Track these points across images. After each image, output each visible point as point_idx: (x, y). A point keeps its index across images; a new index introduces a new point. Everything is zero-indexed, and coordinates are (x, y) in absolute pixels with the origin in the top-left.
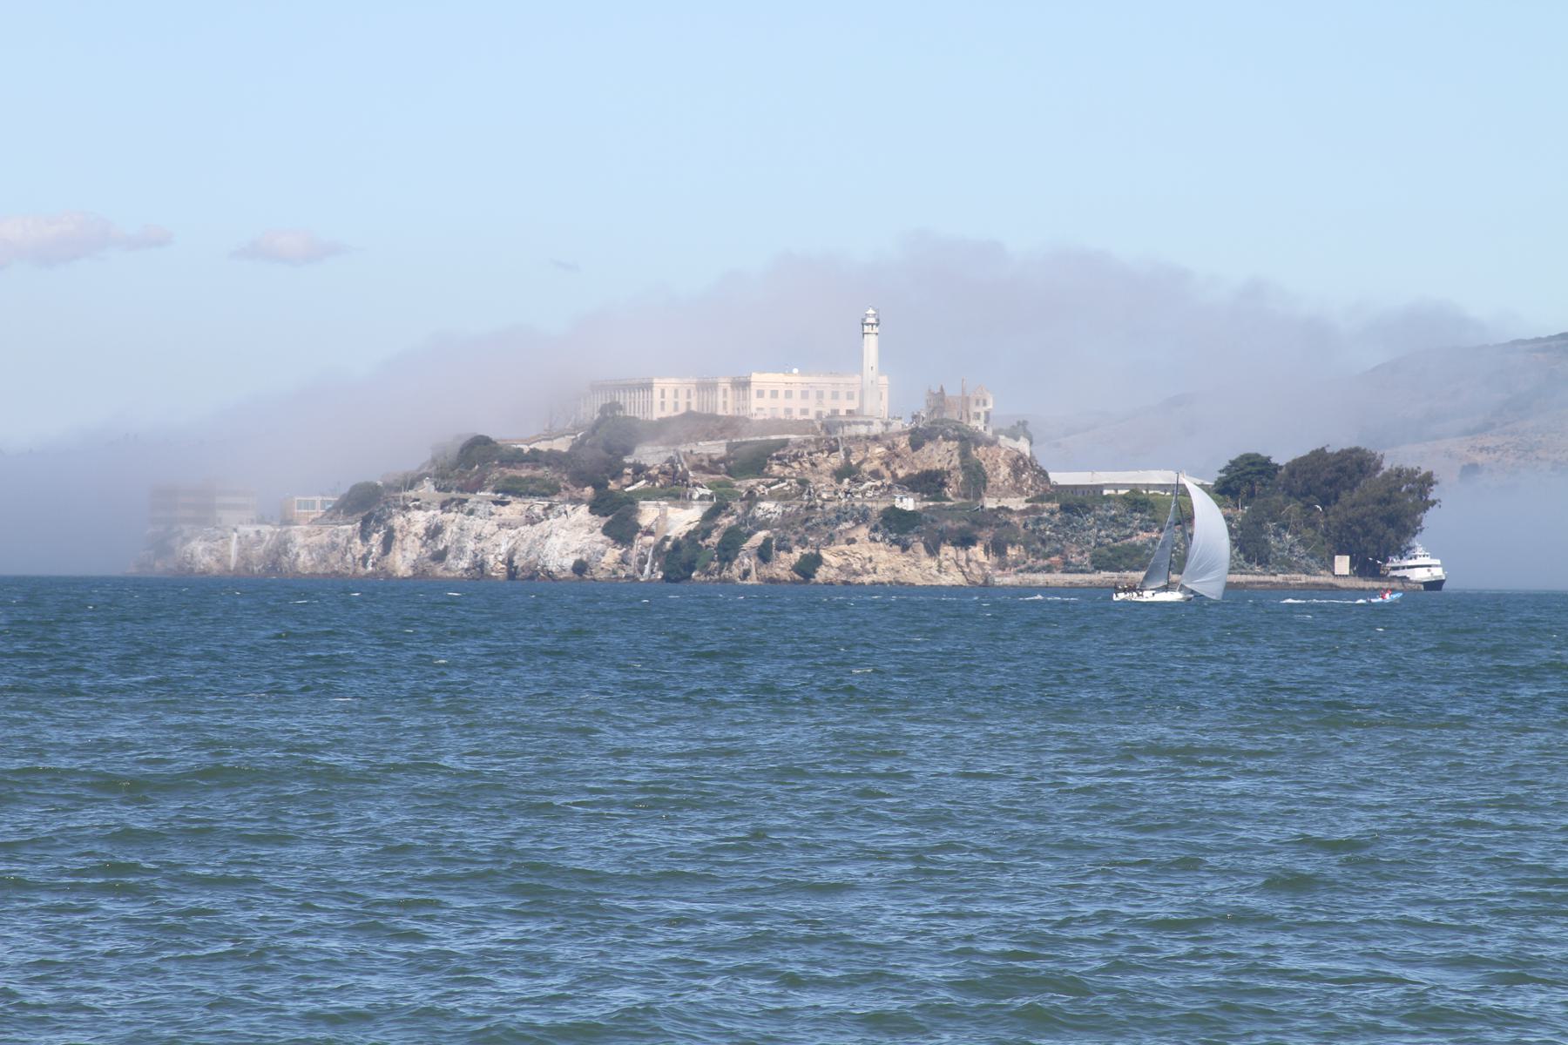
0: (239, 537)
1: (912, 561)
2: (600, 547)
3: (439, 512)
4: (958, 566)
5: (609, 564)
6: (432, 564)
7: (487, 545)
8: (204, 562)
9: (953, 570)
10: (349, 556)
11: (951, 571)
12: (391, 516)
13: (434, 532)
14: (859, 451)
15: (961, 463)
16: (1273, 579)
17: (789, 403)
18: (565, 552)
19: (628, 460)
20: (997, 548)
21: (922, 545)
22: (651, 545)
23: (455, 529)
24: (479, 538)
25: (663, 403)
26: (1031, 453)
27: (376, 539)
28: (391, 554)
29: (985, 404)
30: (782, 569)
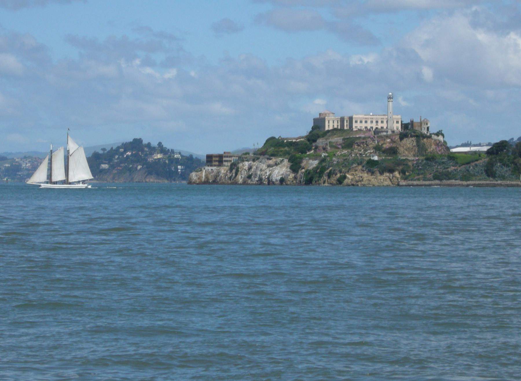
0: (205, 171)
1: (375, 177)
2: (288, 173)
3: (252, 162)
4: (390, 179)
5: (291, 179)
6: (247, 179)
7: (263, 173)
8: (195, 179)
9: (388, 180)
10: (227, 177)
11: (387, 180)
12: (238, 163)
13: (250, 168)
14: (382, 140)
15: (417, 144)
16: (496, 182)
17: (366, 125)
18: (278, 175)
19: (314, 144)
20: (403, 172)
21: (378, 172)
22: (303, 172)
23: (255, 168)
24: (261, 170)
25: (329, 125)
26: (444, 140)
27: (234, 171)
28: (238, 176)
29: (427, 124)
30: (334, 180)
